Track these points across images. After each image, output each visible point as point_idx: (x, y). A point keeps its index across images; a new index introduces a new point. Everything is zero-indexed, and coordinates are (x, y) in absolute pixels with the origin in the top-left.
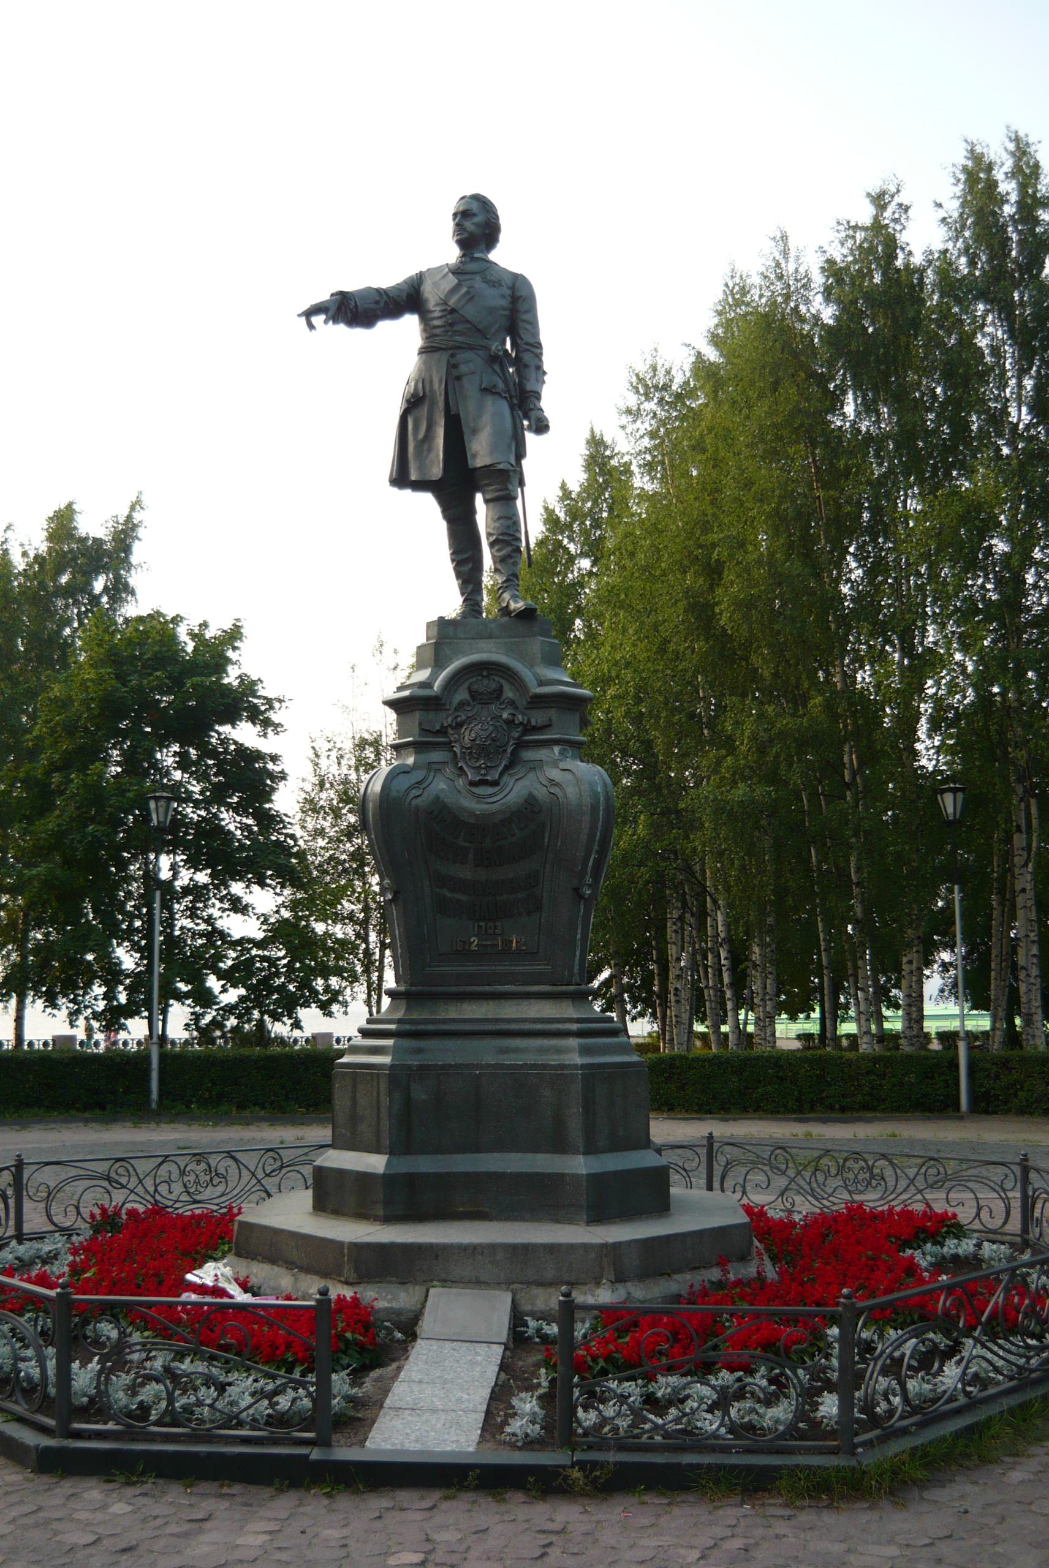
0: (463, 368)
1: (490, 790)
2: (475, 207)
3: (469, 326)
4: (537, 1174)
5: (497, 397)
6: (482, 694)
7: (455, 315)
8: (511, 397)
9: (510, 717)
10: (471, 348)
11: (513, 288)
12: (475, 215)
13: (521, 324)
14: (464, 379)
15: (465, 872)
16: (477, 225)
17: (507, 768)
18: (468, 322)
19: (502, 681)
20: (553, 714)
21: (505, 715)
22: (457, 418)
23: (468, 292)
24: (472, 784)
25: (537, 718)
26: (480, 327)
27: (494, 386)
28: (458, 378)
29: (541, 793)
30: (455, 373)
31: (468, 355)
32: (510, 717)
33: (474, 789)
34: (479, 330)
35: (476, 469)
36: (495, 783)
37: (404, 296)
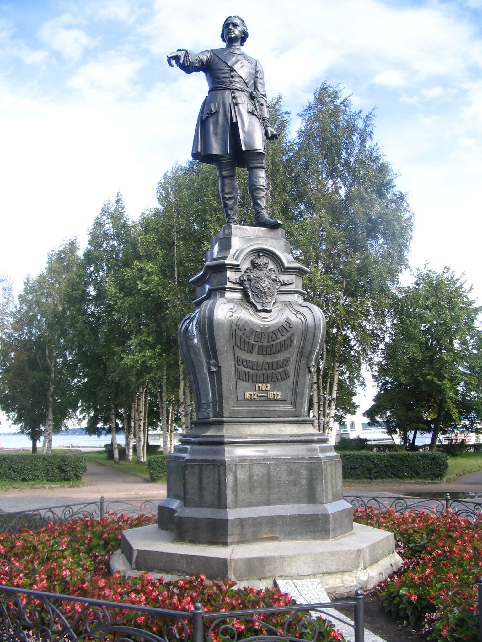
0: (239, 100)
1: (267, 315)
2: (238, 22)
4: (303, 515)
5: (255, 117)
6: (259, 265)
7: (235, 73)
9: (275, 278)
10: (242, 91)
12: (238, 26)
14: (240, 106)
15: (253, 358)
17: (274, 303)
19: (268, 259)
21: (273, 277)
22: (237, 123)
24: (260, 311)
26: (246, 81)
29: (293, 318)
30: (235, 101)
32: (275, 278)
33: (259, 314)
36: (270, 311)
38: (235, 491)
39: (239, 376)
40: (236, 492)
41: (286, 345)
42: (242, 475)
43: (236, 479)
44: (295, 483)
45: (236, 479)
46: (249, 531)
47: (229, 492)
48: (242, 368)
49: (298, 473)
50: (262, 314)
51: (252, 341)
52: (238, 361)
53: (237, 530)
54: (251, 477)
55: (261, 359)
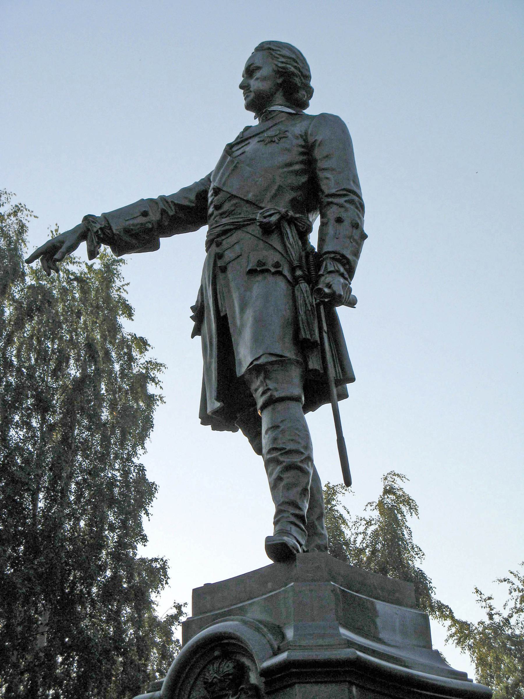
0: (229, 255)
3: (234, 201)
8: (293, 270)
10: (238, 227)
11: (304, 137)
13: (321, 175)
16: (264, 79)
18: (235, 197)
22: (225, 317)
23: (232, 162)
27: (260, 263)
28: (224, 270)
30: (220, 263)
34: (247, 202)
35: (243, 376)
37: (193, 197)
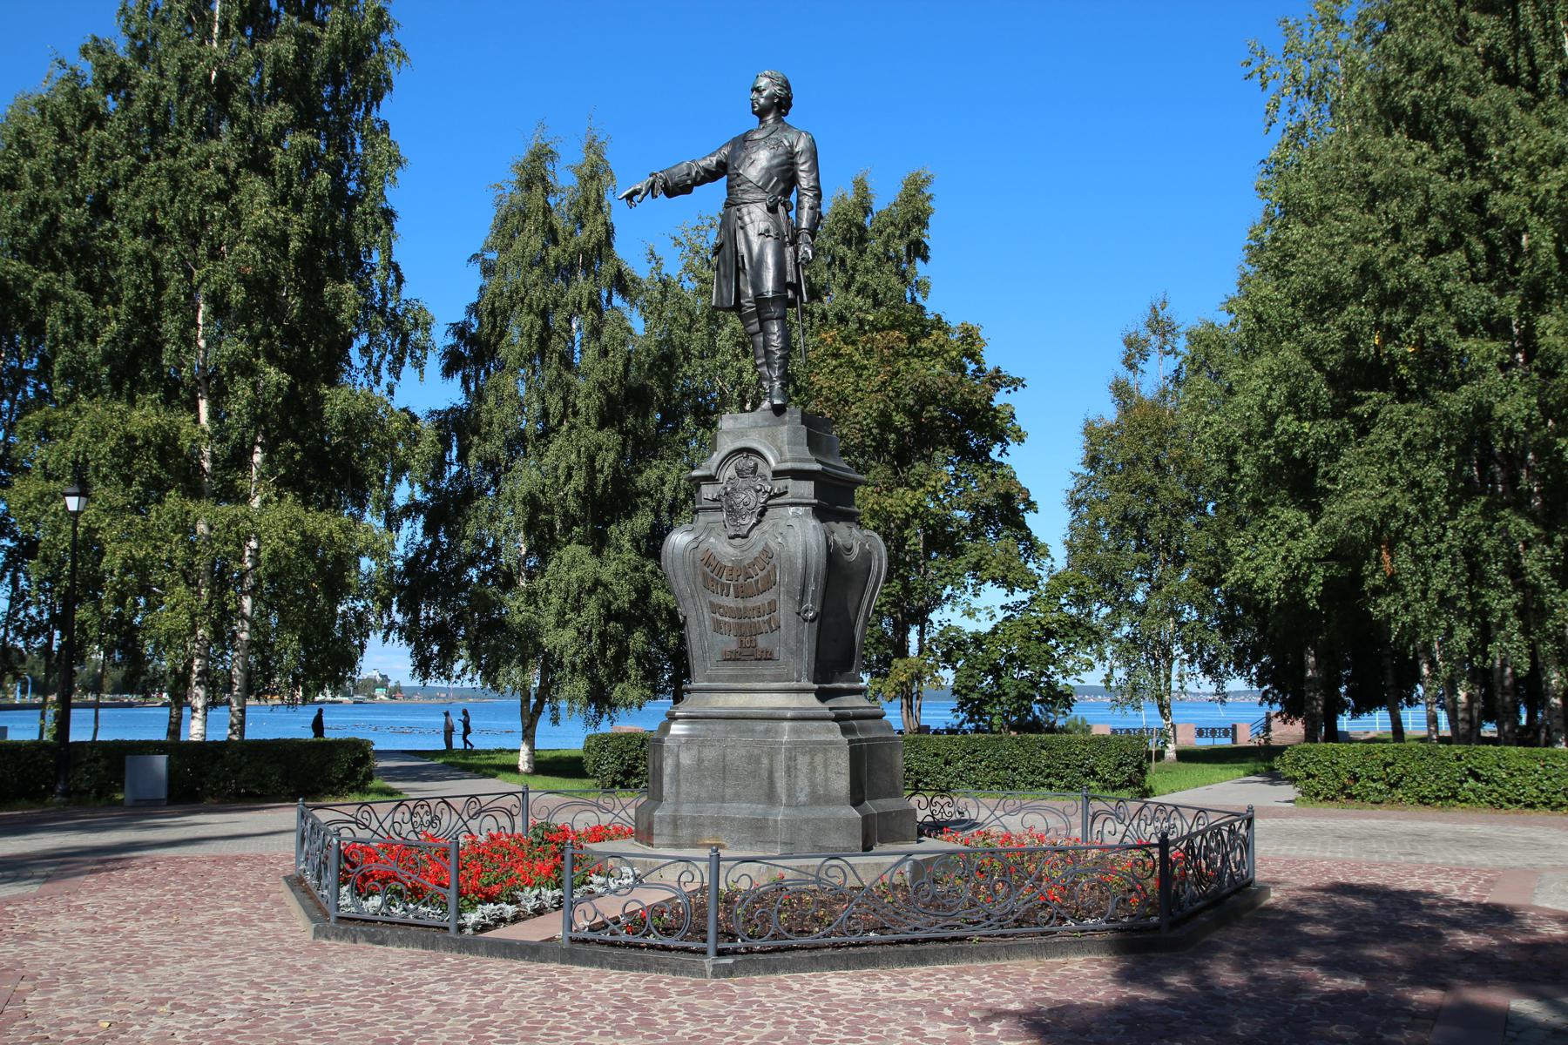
15: (730, 602)
20: (790, 482)
25: (780, 485)
31: (752, 207)
38: (676, 780)
39: (718, 627)
40: (678, 781)
41: (769, 583)
42: (686, 759)
43: (678, 765)
44: (754, 774)
45: (678, 765)
46: (685, 833)
47: (666, 779)
48: (717, 616)
49: (758, 761)
50: (738, 541)
51: (724, 580)
52: (715, 608)
53: (667, 830)
54: (700, 761)
55: (740, 603)
